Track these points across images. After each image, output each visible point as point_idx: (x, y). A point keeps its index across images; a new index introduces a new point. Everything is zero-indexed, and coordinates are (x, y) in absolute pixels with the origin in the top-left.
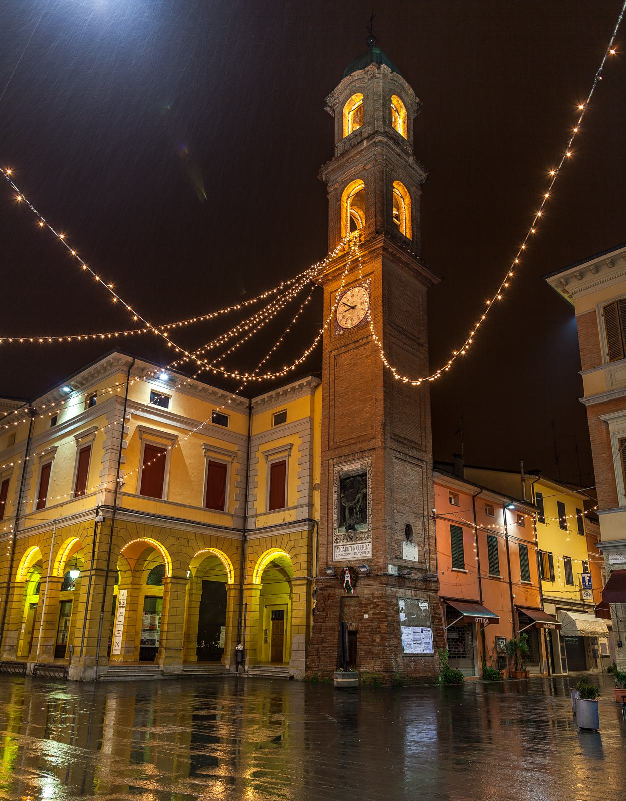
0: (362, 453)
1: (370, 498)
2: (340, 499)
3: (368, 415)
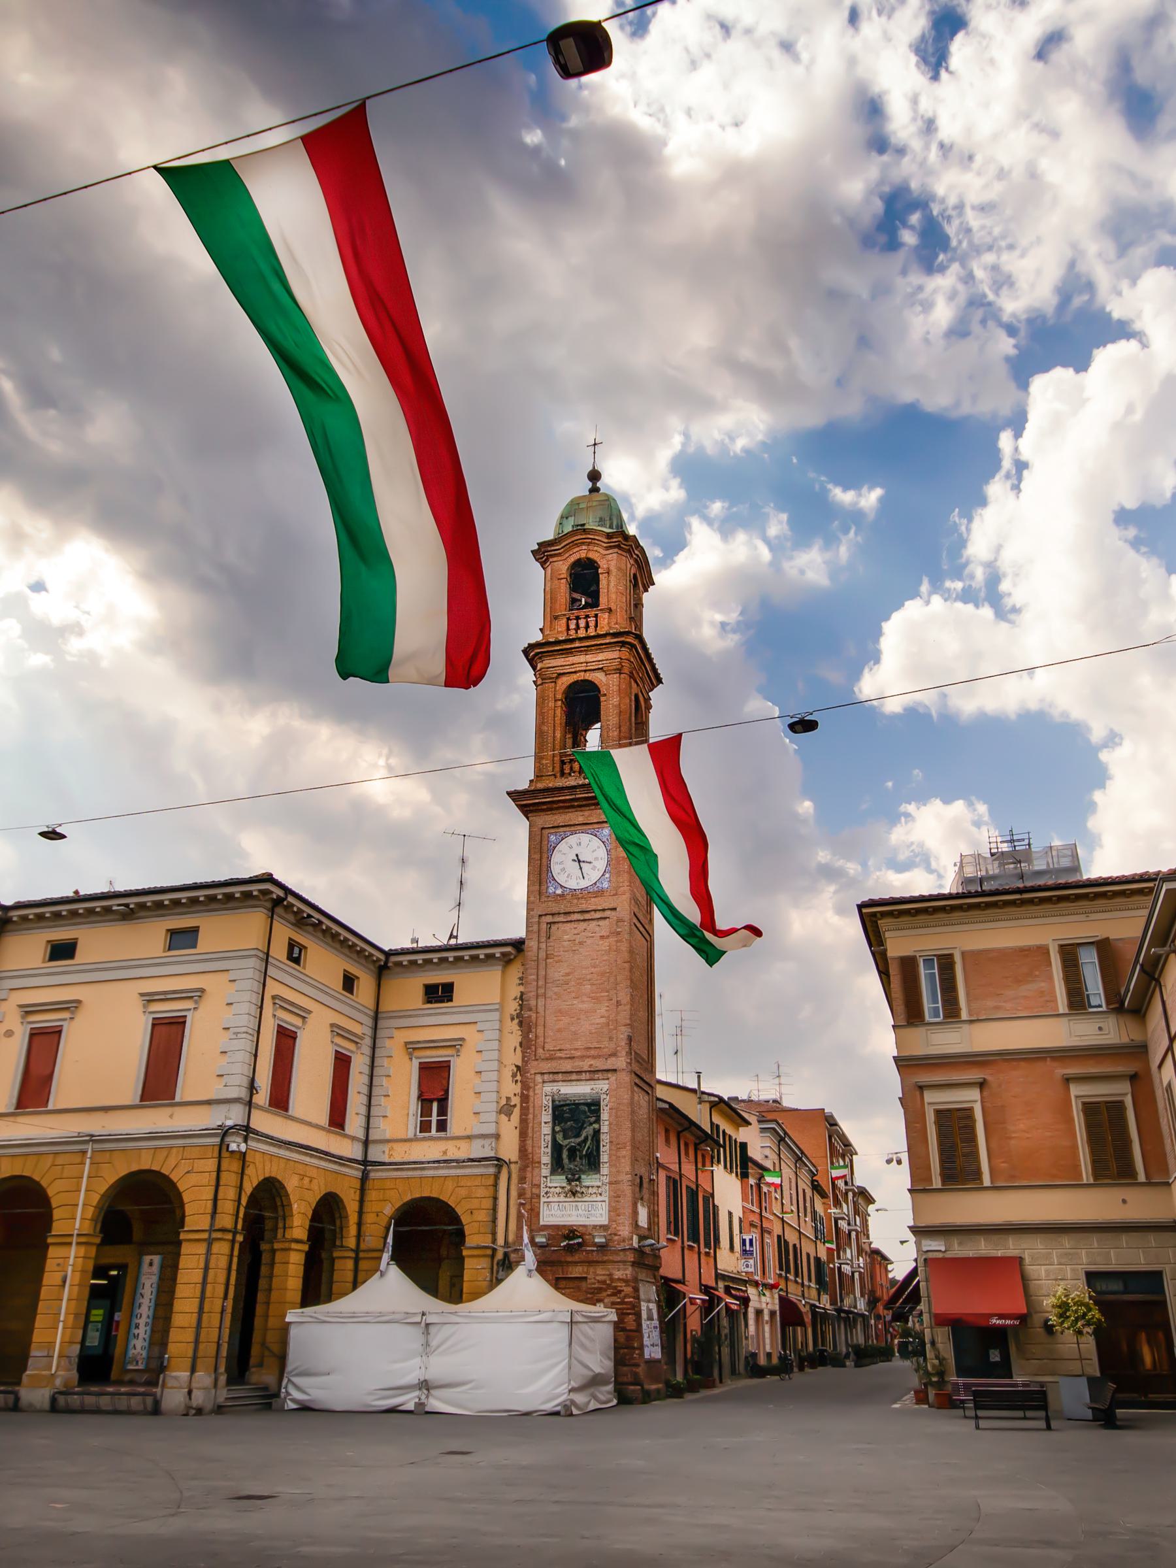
0: (593, 1074)
1: (605, 1139)
2: (554, 1132)
3: (603, 1020)
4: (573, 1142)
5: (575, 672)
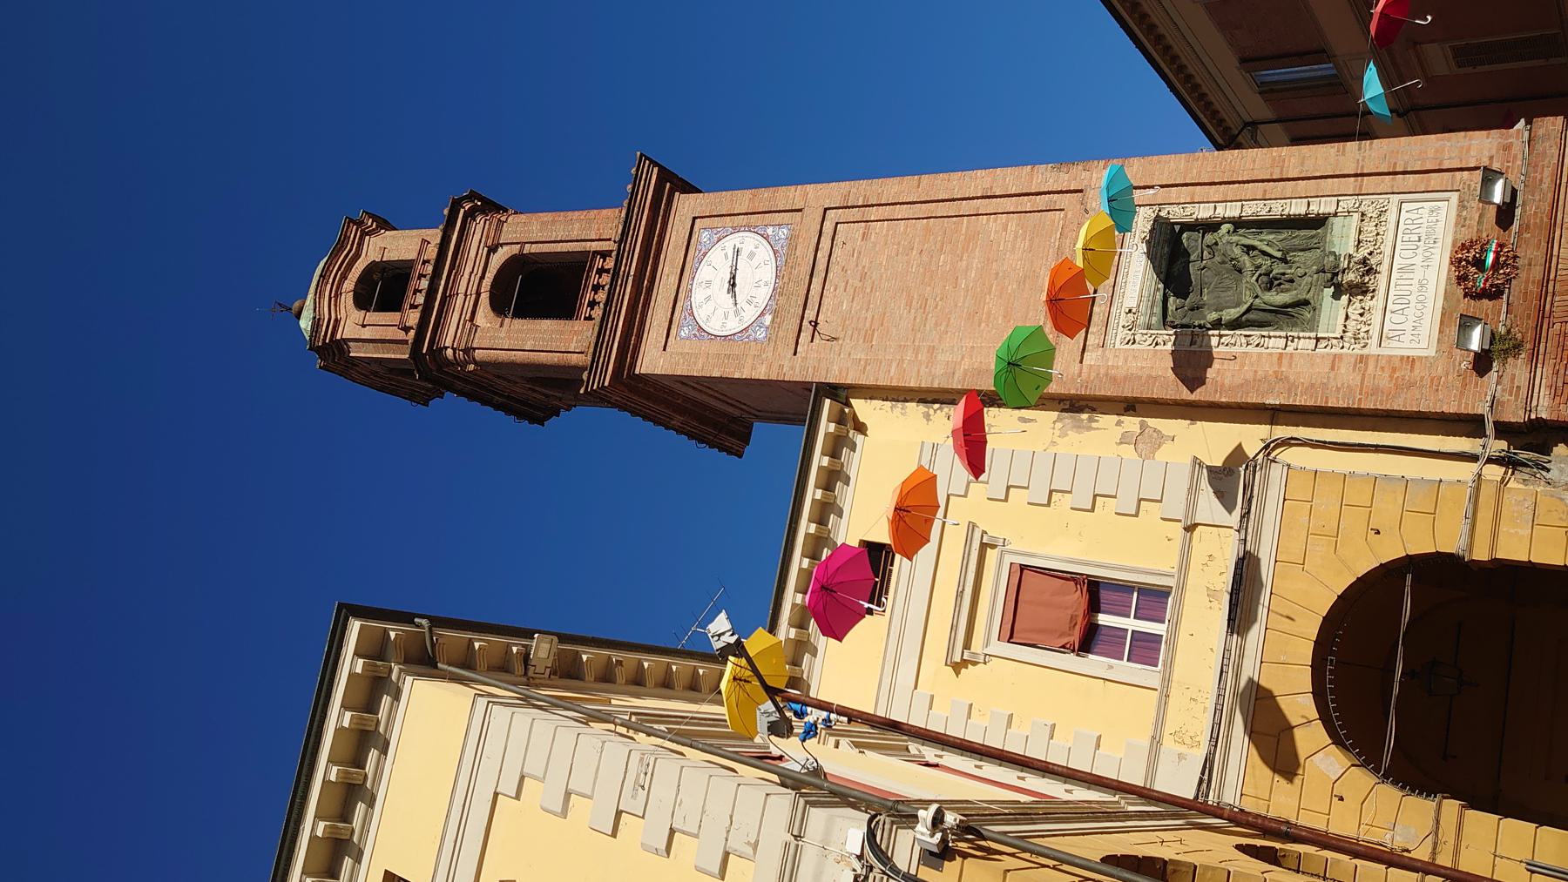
5: (478, 294)
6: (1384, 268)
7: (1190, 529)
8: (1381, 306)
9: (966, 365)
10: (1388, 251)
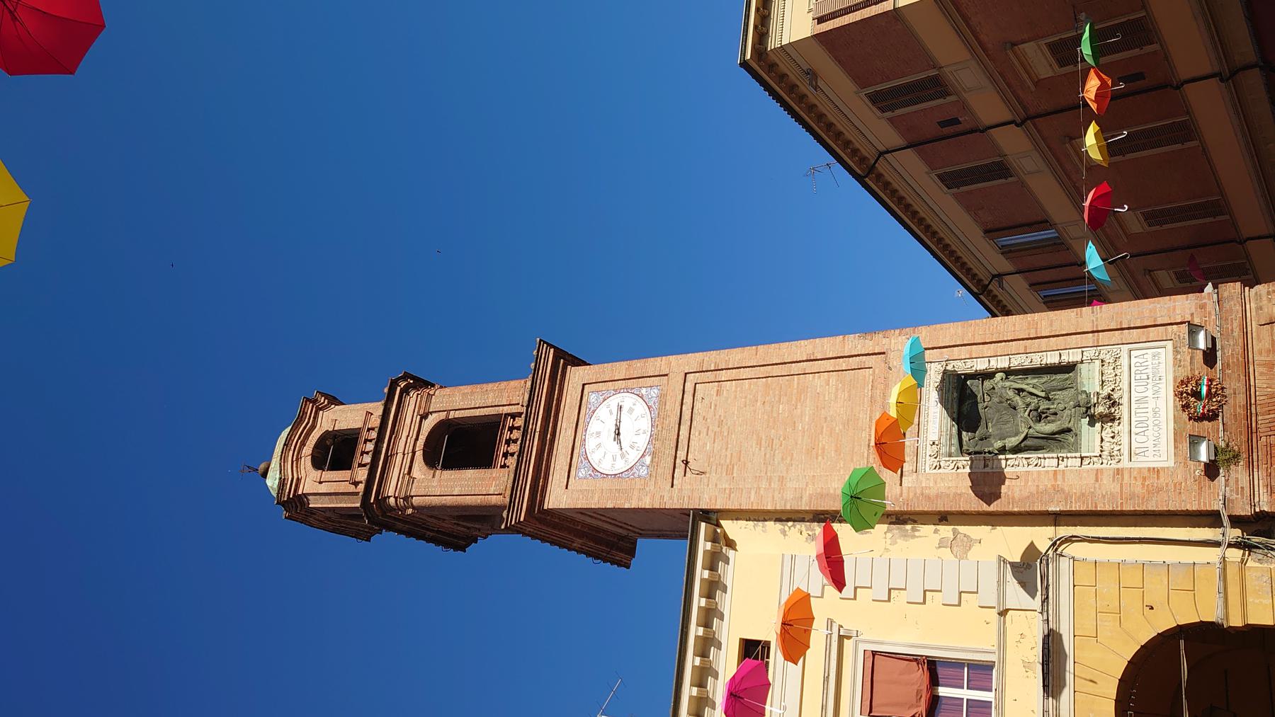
4: (1023, 414)
5: (414, 453)
6: (1125, 401)
7: (1003, 613)
8: (1127, 430)
9: (810, 490)
10: (1126, 388)
